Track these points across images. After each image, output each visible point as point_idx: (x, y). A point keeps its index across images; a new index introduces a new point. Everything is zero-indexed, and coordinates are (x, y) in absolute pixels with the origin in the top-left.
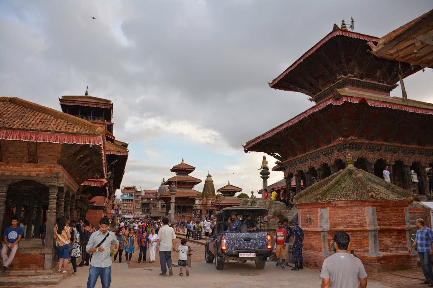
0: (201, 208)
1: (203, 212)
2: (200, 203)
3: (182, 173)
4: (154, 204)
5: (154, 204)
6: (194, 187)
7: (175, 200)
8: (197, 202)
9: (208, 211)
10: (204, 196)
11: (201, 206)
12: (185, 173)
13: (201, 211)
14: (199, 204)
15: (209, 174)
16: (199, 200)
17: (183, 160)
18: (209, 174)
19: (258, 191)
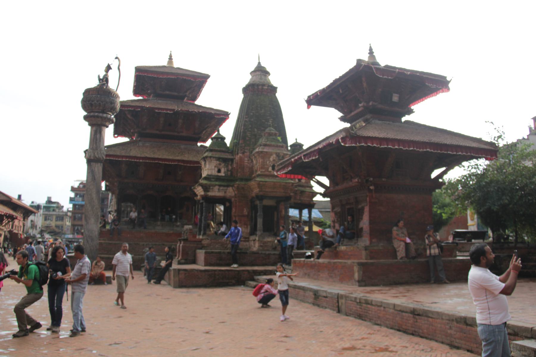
2: (222, 174)
11: (228, 186)
14: (218, 178)
15: (259, 63)
16: (218, 159)
17: (171, 58)
18: (259, 63)
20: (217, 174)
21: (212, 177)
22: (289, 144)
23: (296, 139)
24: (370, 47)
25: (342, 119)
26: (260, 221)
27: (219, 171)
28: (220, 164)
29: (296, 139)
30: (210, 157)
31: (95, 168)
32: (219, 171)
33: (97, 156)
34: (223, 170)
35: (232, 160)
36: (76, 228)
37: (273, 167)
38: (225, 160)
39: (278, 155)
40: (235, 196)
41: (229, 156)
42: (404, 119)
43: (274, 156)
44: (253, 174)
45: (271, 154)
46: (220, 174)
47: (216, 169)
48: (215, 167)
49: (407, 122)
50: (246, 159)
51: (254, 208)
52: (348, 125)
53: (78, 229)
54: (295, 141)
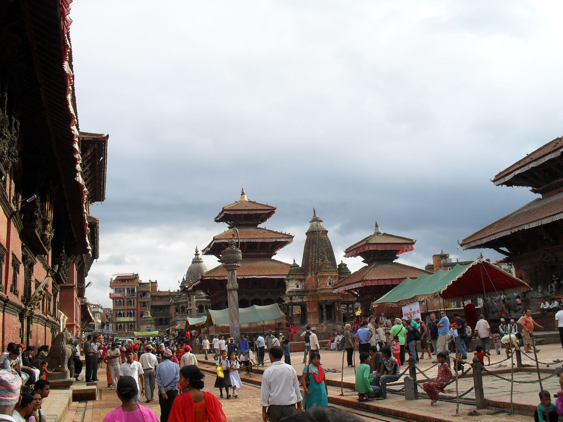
0: (304, 300)
1: (308, 310)
2: (299, 288)
3: (245, 222)
4: (181, 305)
5: (181, 305)
6: (275, 254)
7: (237, 284)
8: (292, 286)
9: (324, 306)
10: (309, 268)
12: (251, 223)
13: (303, 309)
14: (297, 291)
16: (297, 280)
19: (461, 242)
20: (296, 288)
21: (294, 291)
22: (337, 265)
23: (342, 261)
24: (376, 223)
25: (364, 261)
26: (325, 314)
27: (298, 287)
28: (298, 282)
29: (342, 261)
30: (292, 279)
31: (234, 294)
32: (298, 287)
33: (234, 287)
34: (299, 286)
35: (305, 279)
36: (119, 325)
37: (330, 284)
38: (301, 280)
39: (332, 276)
40: (309, 301)
41: (302, 277)
42: (394, 262)
43: (330, 277)
44: (318, 287)
45: (328, 276)
46: (298, 289)
47: (296, 286)
48: (295, 284)
49: (395, 263)
50: (313, 279)
51: (321, 307)
52: (367, 265)
53: (121, 326)
54: (341, 262)
